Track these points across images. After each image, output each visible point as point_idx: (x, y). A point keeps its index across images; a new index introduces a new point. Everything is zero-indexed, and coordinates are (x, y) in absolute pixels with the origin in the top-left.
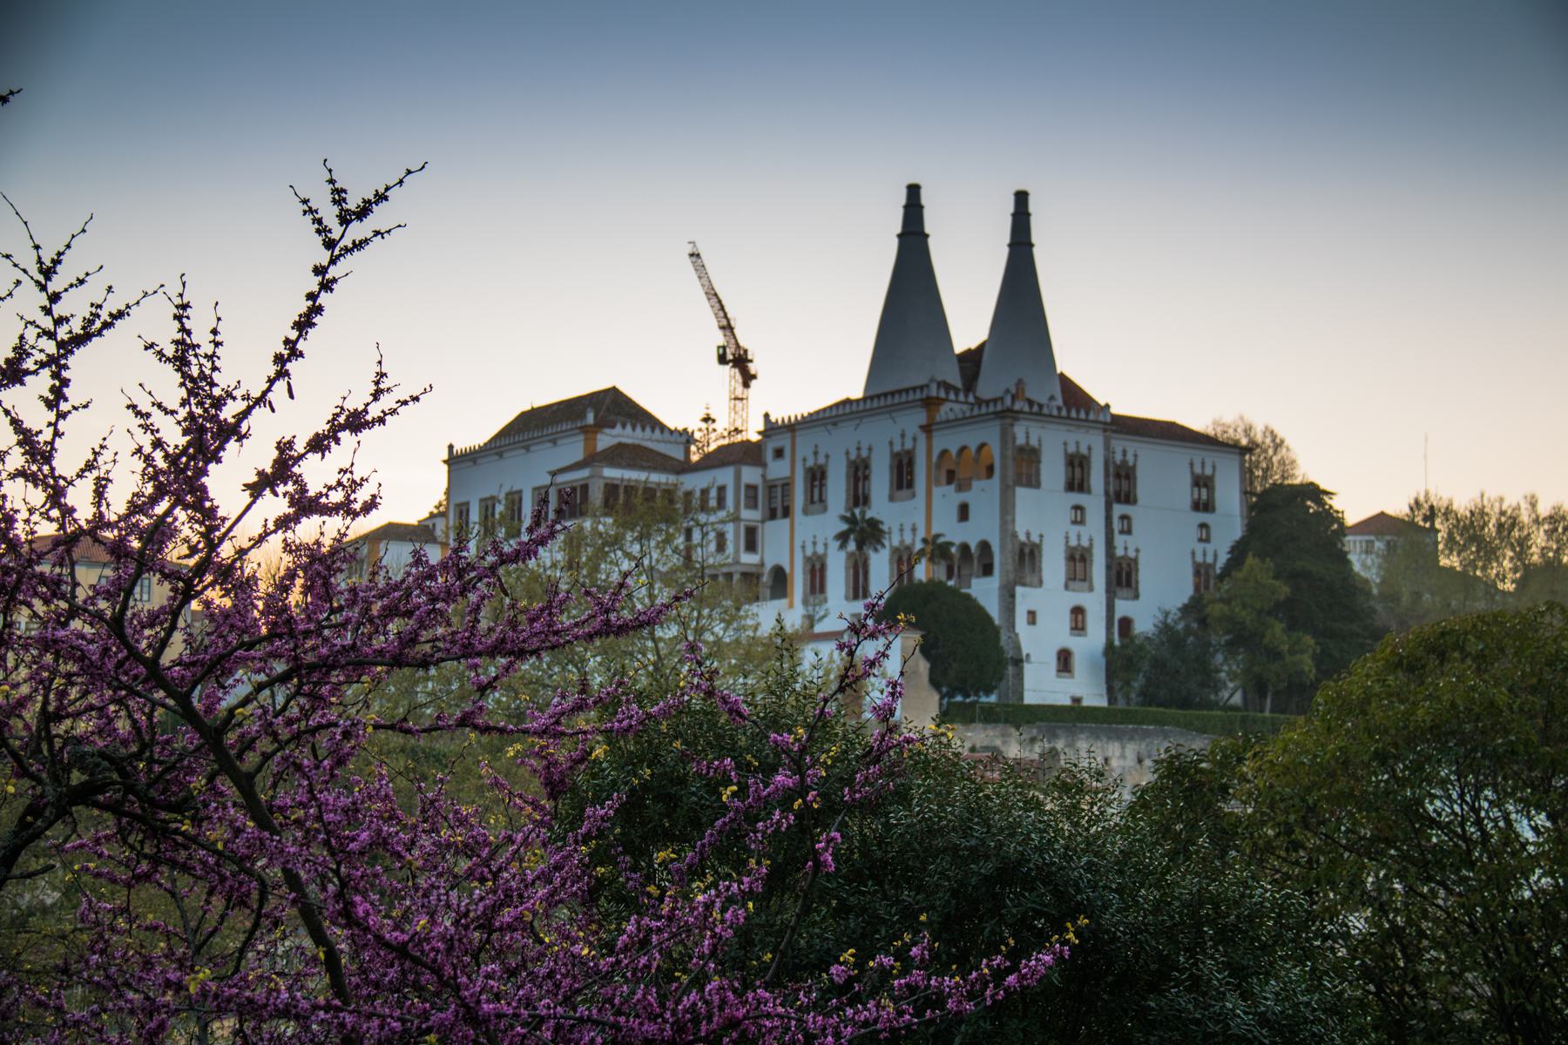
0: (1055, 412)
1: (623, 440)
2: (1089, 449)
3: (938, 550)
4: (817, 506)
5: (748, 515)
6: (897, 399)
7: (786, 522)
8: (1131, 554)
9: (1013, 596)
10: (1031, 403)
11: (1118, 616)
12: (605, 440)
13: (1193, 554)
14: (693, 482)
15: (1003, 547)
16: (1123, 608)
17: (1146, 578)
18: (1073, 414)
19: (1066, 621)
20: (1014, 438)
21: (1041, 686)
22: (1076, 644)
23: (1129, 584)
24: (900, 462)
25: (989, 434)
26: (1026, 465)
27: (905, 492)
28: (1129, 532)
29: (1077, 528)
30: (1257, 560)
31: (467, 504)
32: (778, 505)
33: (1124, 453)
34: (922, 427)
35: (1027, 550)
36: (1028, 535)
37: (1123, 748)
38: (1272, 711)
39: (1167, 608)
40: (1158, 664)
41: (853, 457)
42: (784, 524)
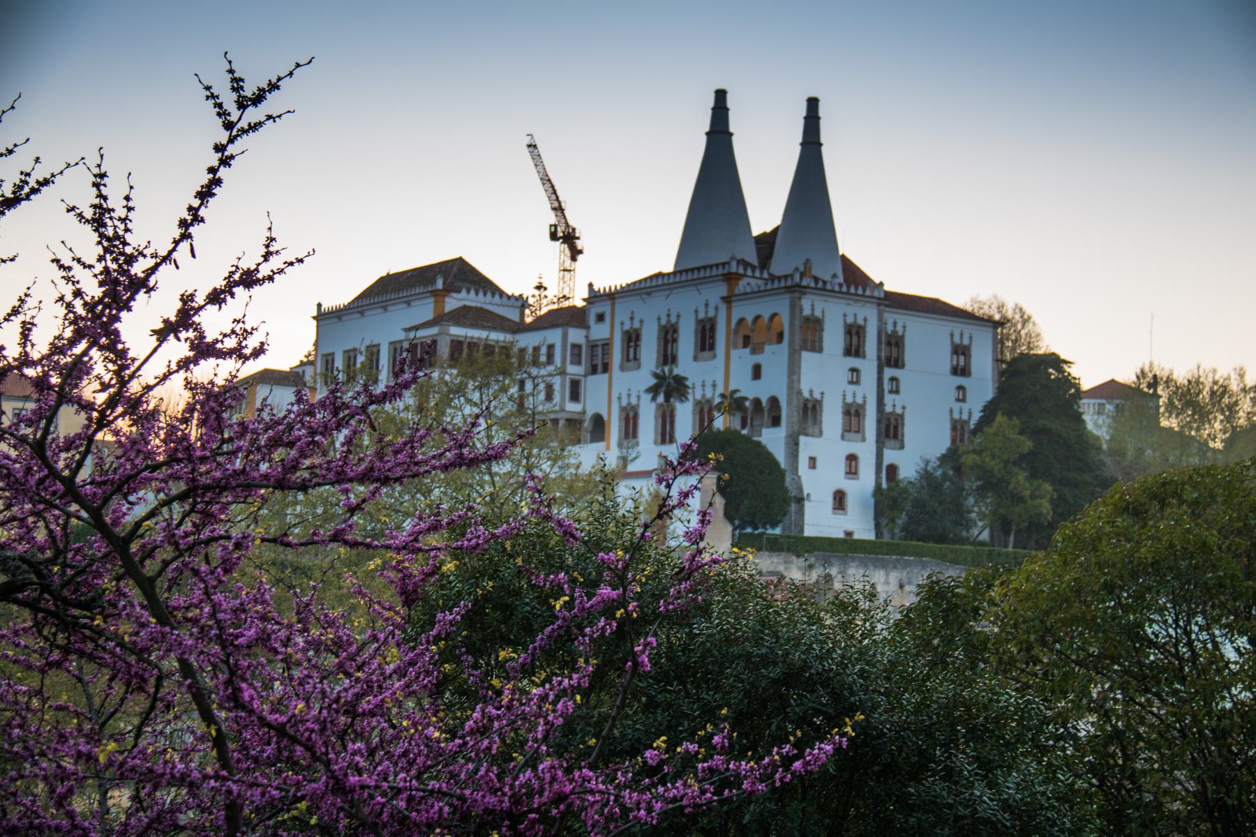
0: (837, 288)
1: (468, 303)
2: (865, 320)
3: (734, 403)
4: (632, 364)
5: (574, 370)
6: (702, 274)
7: (606, 376)
8: (899, 411)
9: (797, 444)
10: (816, 279)
11: (886, 462)
12: (453, 303)
13: (951, 411)
14: (527, 341)
15: (789, 403)
16: (890, 456)
17: (910, 431)
18: (852, 290)
19: (842, 466)
20: (802, 310)
21: (819, 521)
22: (849, 486)
23: (895, 437)
24: (704, 327)
25: (780, 305)
26: (810, 334)
27: (707, 354)
28: (897, 392)
29: (853, 387)
30: (1005, 418)
31: (333, 354)
32: (599, 362)
33: (895, 324)
34: (723, 298)
35: (810, 406)
36: (811, 392)
37: (887, 575)
38: (1015, 547)
39: (928, 457)
40: (919, 504)
41: (664, 322)
42: (602, 378)
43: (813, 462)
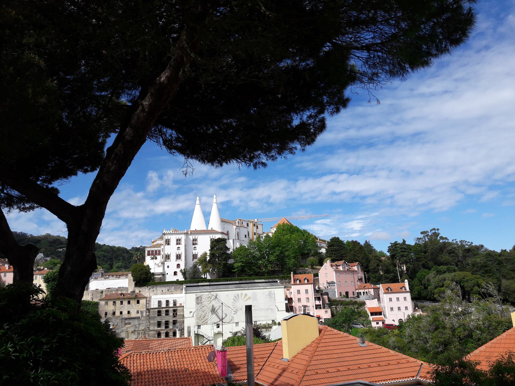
21: (170, 278)
22: (178, 270)
43: (168, 267)
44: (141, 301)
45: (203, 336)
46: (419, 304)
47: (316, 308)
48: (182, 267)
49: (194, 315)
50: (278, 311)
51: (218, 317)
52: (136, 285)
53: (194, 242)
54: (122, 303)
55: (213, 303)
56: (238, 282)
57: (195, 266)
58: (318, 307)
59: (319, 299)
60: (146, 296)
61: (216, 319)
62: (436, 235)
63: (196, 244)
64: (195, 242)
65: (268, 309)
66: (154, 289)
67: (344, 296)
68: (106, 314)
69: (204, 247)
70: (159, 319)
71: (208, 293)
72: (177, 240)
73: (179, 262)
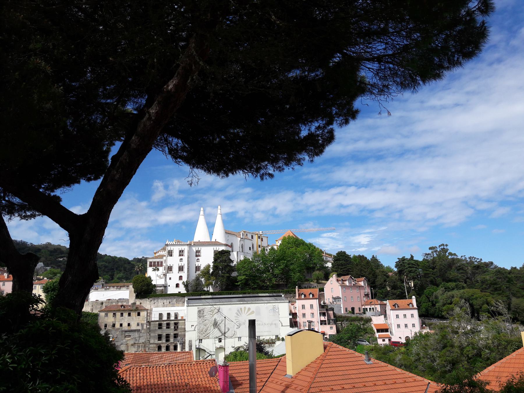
21: (172, 290)
22: (180, 283)
43: (170, 279)
44: (142, 314)
45: (205, 351)
46: (427, 321)
47: (321, 324)
48: (185, 279)
49: (196, 329)
50: (282, 326)
51: (220, 331)
52: (137, 297)
53: (197, 254)
54: (122, 315)
55: (216, 316)
56: (241, 296)
57: (197, 279)
58: (322, 323)
59: (324, 314)
60: (147, 308)
61: (217, 333)
62: (445, 251)
63: (199, 256)
64: (198, 254)
65: (271, 324)
66: (156, 301)
67: (350, 312)
68: (106, 326)
69: (207, 259)
70: (159, 332)
71: (210, 307)
72: (180, 251)
73: (181, 274)
